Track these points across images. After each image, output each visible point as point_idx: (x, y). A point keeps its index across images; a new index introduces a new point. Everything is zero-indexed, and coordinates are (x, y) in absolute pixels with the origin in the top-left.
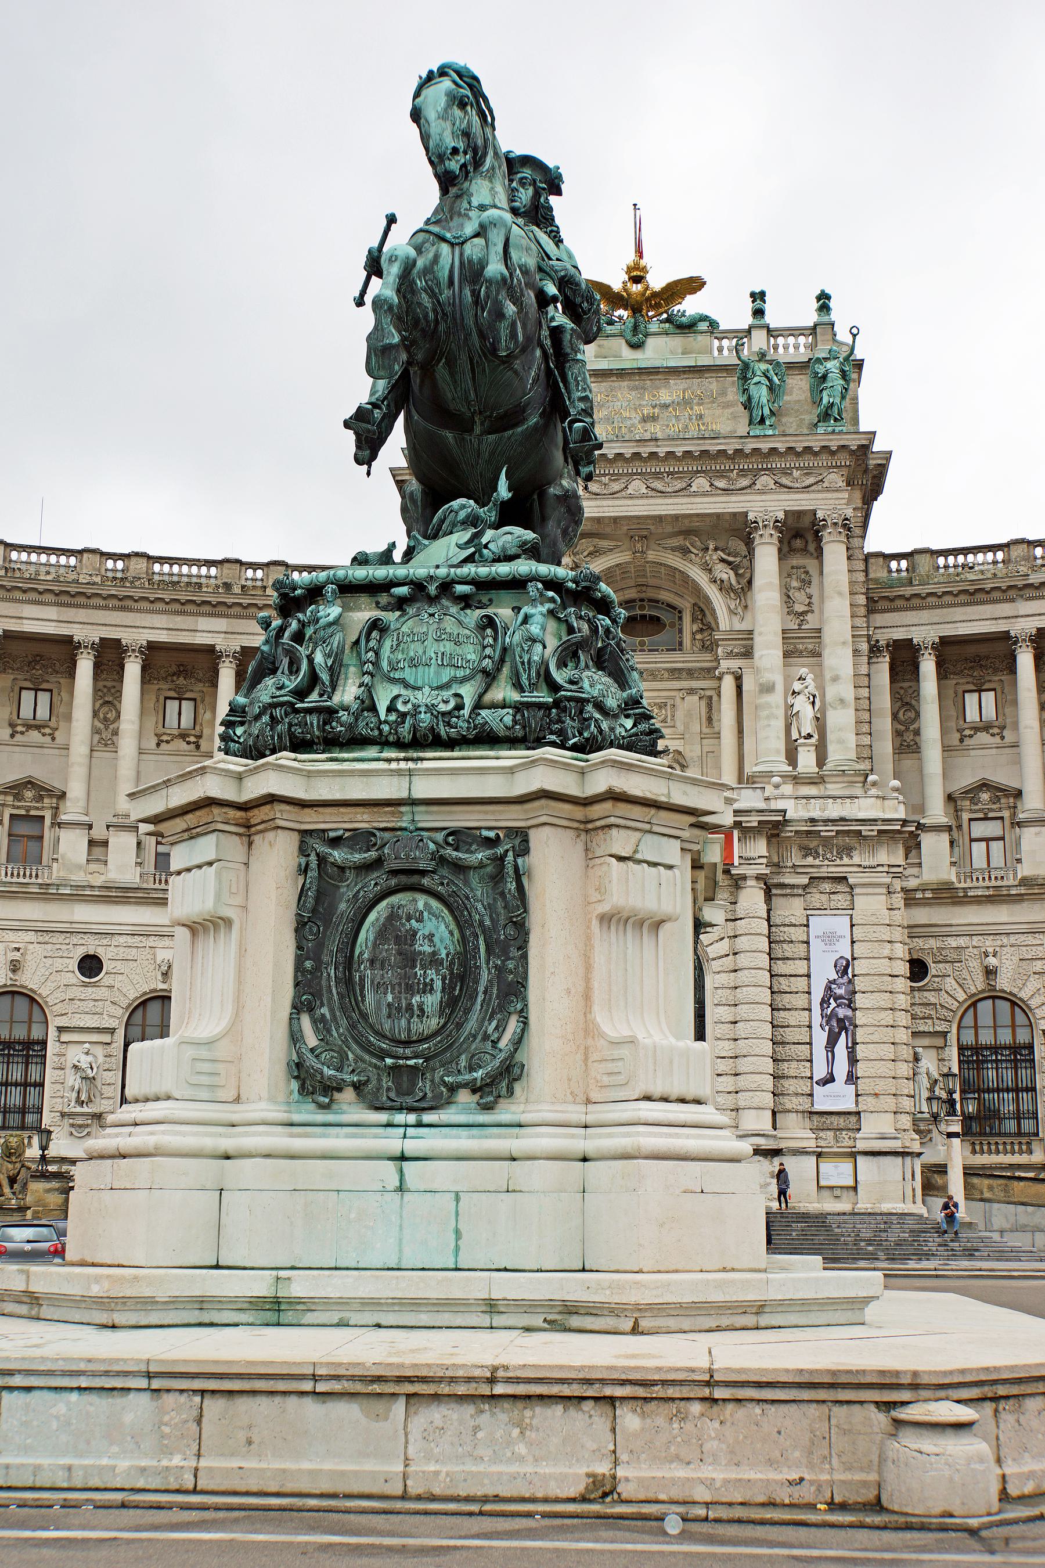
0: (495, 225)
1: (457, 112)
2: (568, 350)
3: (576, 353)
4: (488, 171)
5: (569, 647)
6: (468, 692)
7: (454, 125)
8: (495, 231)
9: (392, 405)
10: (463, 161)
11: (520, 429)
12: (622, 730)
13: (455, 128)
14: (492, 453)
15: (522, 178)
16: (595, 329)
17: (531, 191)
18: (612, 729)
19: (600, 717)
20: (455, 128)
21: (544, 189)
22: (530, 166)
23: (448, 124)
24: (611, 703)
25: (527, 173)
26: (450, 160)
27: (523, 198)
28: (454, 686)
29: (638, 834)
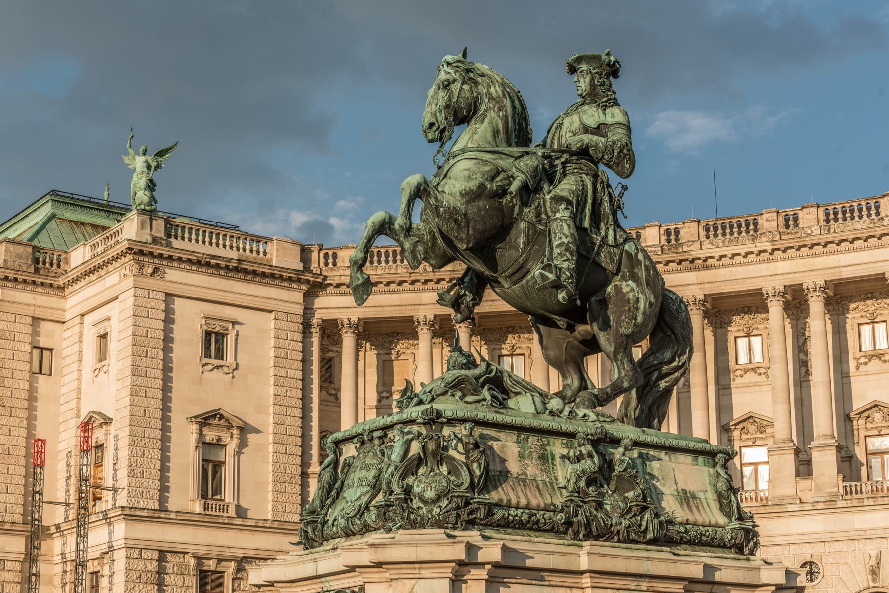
1: (441, 93)
2: (550, 214)
3: (555, 213)
4: (482, 114)
5: (411, 463)
6: (364, 500)
9: (474, 278)
10: (442, 127)
11: (530, 277)
12: (438, 510)
14: (525, 294)
16: (627, 166)
17: (588, 80)
18: (430, 512)
19: (421, 505)
23: (433, 105)
24: (430, 494)
25: (584, 67)
28: (362, 497)
29: (413, 581)
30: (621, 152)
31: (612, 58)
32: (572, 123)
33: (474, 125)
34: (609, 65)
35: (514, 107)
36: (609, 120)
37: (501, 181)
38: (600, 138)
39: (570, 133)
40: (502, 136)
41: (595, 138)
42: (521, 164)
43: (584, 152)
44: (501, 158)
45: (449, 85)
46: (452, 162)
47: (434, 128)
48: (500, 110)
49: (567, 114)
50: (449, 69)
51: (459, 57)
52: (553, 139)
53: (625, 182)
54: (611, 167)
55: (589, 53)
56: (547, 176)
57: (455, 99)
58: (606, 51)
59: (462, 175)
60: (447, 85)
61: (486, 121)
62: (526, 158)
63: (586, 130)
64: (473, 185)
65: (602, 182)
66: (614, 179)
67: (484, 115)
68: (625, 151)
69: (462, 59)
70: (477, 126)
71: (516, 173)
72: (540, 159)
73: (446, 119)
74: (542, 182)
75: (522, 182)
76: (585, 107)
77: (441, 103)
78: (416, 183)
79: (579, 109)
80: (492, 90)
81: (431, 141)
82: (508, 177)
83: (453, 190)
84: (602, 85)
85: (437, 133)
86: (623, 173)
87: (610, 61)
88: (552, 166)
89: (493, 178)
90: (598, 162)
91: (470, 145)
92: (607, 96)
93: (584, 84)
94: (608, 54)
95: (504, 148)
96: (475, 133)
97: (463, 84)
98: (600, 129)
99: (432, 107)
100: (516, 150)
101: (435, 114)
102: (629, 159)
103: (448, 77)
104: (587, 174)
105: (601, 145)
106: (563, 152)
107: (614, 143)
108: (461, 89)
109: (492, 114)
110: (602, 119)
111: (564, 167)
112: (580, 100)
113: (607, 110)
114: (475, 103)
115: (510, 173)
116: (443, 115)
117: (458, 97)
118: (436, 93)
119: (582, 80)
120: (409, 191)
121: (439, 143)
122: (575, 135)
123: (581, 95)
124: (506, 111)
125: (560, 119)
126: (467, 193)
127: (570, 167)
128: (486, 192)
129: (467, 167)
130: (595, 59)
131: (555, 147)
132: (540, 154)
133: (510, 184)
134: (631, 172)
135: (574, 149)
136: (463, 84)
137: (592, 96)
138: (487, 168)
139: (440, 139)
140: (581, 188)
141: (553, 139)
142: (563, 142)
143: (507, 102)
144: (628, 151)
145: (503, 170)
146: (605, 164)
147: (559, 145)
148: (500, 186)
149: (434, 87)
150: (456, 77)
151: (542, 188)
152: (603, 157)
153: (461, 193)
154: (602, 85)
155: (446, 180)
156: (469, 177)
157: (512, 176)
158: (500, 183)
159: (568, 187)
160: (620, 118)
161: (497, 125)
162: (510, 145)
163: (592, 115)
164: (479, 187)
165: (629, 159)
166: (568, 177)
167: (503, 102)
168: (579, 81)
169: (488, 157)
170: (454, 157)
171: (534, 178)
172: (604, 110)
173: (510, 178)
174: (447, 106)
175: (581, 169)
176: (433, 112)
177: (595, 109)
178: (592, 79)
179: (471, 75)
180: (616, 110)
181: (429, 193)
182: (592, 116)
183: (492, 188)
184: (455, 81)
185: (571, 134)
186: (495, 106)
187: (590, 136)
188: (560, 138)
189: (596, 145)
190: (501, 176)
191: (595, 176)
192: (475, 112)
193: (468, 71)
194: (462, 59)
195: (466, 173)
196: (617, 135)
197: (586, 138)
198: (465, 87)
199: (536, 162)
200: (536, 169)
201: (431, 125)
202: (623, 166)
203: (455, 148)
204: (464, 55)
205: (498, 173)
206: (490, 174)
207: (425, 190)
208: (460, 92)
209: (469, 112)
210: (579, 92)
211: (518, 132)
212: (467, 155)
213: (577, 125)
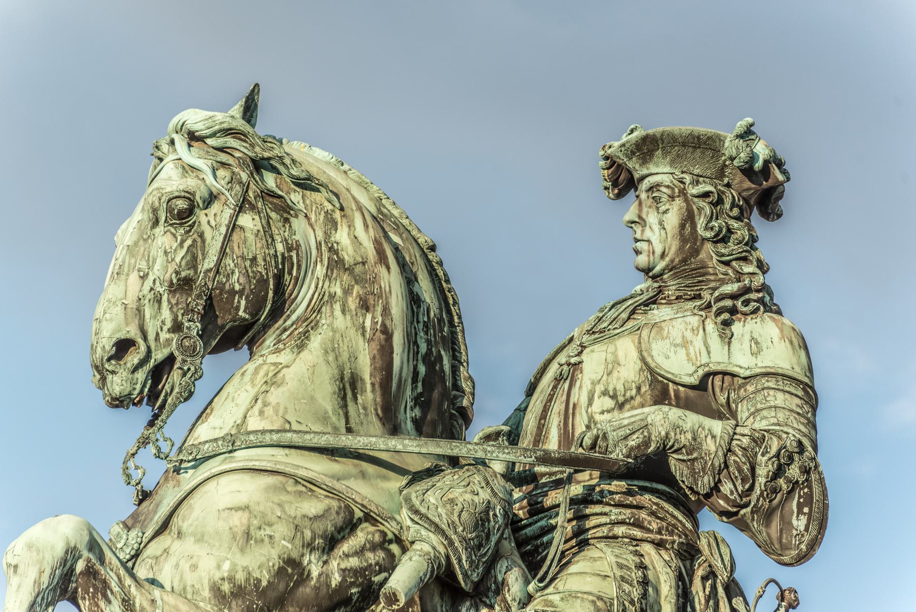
0: (16, 567)
1: (164, 239)
4: (303, 319)
7: (143, 278)
8: (15, 580)
10: (159, 355)
13: (148, 283)
15: (650, 189)
16: (800, 523)
20: (148, 283)
21: (706, 195)
22: (665, 154)
23: (134, 278)
25: (660, 172)
26: (113, 372)
27: (653, 240)
30: (779, 472)
31: (761, 150)
32: (612, 364)
33: (270, 353)
34: (748, 171)
35: (414, 300)
36: (741, 359)
37: (360, 552)
38: (708, 422)
39: (606, 395)
40: (369, 396)
41: (692, 419)
42: (432, 498)
43: (650, 469)
44: (363, 475)
45: (190, 211)
46: (189, 478)
47: (133, 358)
48: (365, 306)
49: (598, 333)
50: (192, 157)
51: (233, 116)
52: (544, 415)
53: (788, 577)
54: (743, 526)
55: (681, 127)
56: (520, 545)
57: (209, 262)
58: (740, 125)
59: (223, 526)
60: (183, 213)
61: (316, 342)
62: (449, 478)
63: (661, 390)
64: (259, 563)
65: (711, 574)
66: (753, 566)
67: (310, 323)
68: (794, 472)
69: (240, 124)
70: (284, 357)
71: (412, 530)
72: (500, 484)
73: (177, 327)
74: (502, 565)
75: (433, 561)
76: (660, 313)
77: (162, 271)
78: (59, 550)
79: (640, 319)
80: (342, 236)
81: (119, 402)
82: (383, 544)
83: (190, 579)
84: (722, 238)
85: (141, 375)
86: (785, 547)
87: (753, 158)
88: (536, 509)
89: (331, 543)
90: (700, 505)
91: (254, 423)
92: (739, 276)
93: (660, 232)
94: (747, 134)
95: (371, 438)
96: (273, 381)
97: (240, 209)
98: (706, 393)
99: (129, 281)
100: (413, 449)
101: (139, 311)
102: (808, 500)
103: (191, 183)
104: (659, 545)
105: (710, 446)
106: (579, 464)
107: (758, 440)
108: (233, 227)
109: (337, 321)
110: (719, 358)
111: (580, 517)
112: (643, 285)
113: (737, 327)
114: (279, 278)
115: (390, 528)
116: (166, 314)
117: (223, 253)
118: (145, 238)
119: (652, 218)
120: (32, 574)
121: (145, 412)
122: (621, 406)
123: (646, 270)
124: (386, 311)
125: (572, 349)
126: (239, 592)
127: (599, 518)
128: (306, 591)
129: (242, 499)
130: (703, 145)
131: (552, 444)
132: (498, 467)
133: (390, 566)
134: (814, 545)
135: (618, 454)
136: (240, 209)
137: (682, 277)
138: (313, 507)
139: (153, 395)
140: (636, 594)
141: (544, 415)
142: (580, 428)
143: (391, 281)
144: (806, 471)
145: (368, 518)
146: (723, 513)
147: (566, 437)
148: (355, 572)
149: (139, 215)
150: (217, 186)
151: (500, 587)
152: (716, 488)
153: (216, 590)
154: (722, 238)
155: (164, 541)
156: (248, 535)
157: (398, 540)
158: (354, 562)
159: (591, 585)
160: (780, 356)
161: (353, 358)
162: (394, 430)
163: (683, 343)
164: (281, 572)
165: (808, 500)
166: (591, 552)
167: (375, 280)
168: (641, 221)
169: (317, 467)
170: (199, 462)
171: (475, 547)
172: (727, 324)
173: (392, 546)
174: (183, 285)
175: (638, 524)
176: (131, 301)
177: (695, 321)
178: (689, 218)
179: (270, 180)
180: (765, 328)
181: (106, 584)
182: (685, 344)
183: (325, 576)
184: (211, 198)
185: (609, 403)
186: (347, 292)
187: (674, 413)
188: (568, 413)
189: (695, 446)
190: (361, 537)
191: (689, 553)
192: (278, 311)
193: (259, 165)
194: (240, 124)
195: (239, 520)
196: (770, 415)
197: (662, 420)
198: (247, 220)
199: (485, 495)
200: (482, 520)
201: (123, 346)
202: (786, 524)
203: (204, 432)
204: (250, 110)
205: (350, 526)
206: (320, 527)
207: (90, 572)
208: (228, 238)
209: (256, 307)
210: (642, 260)
211: (426, 388)
212: (243, 457)
213: (629, 372)
